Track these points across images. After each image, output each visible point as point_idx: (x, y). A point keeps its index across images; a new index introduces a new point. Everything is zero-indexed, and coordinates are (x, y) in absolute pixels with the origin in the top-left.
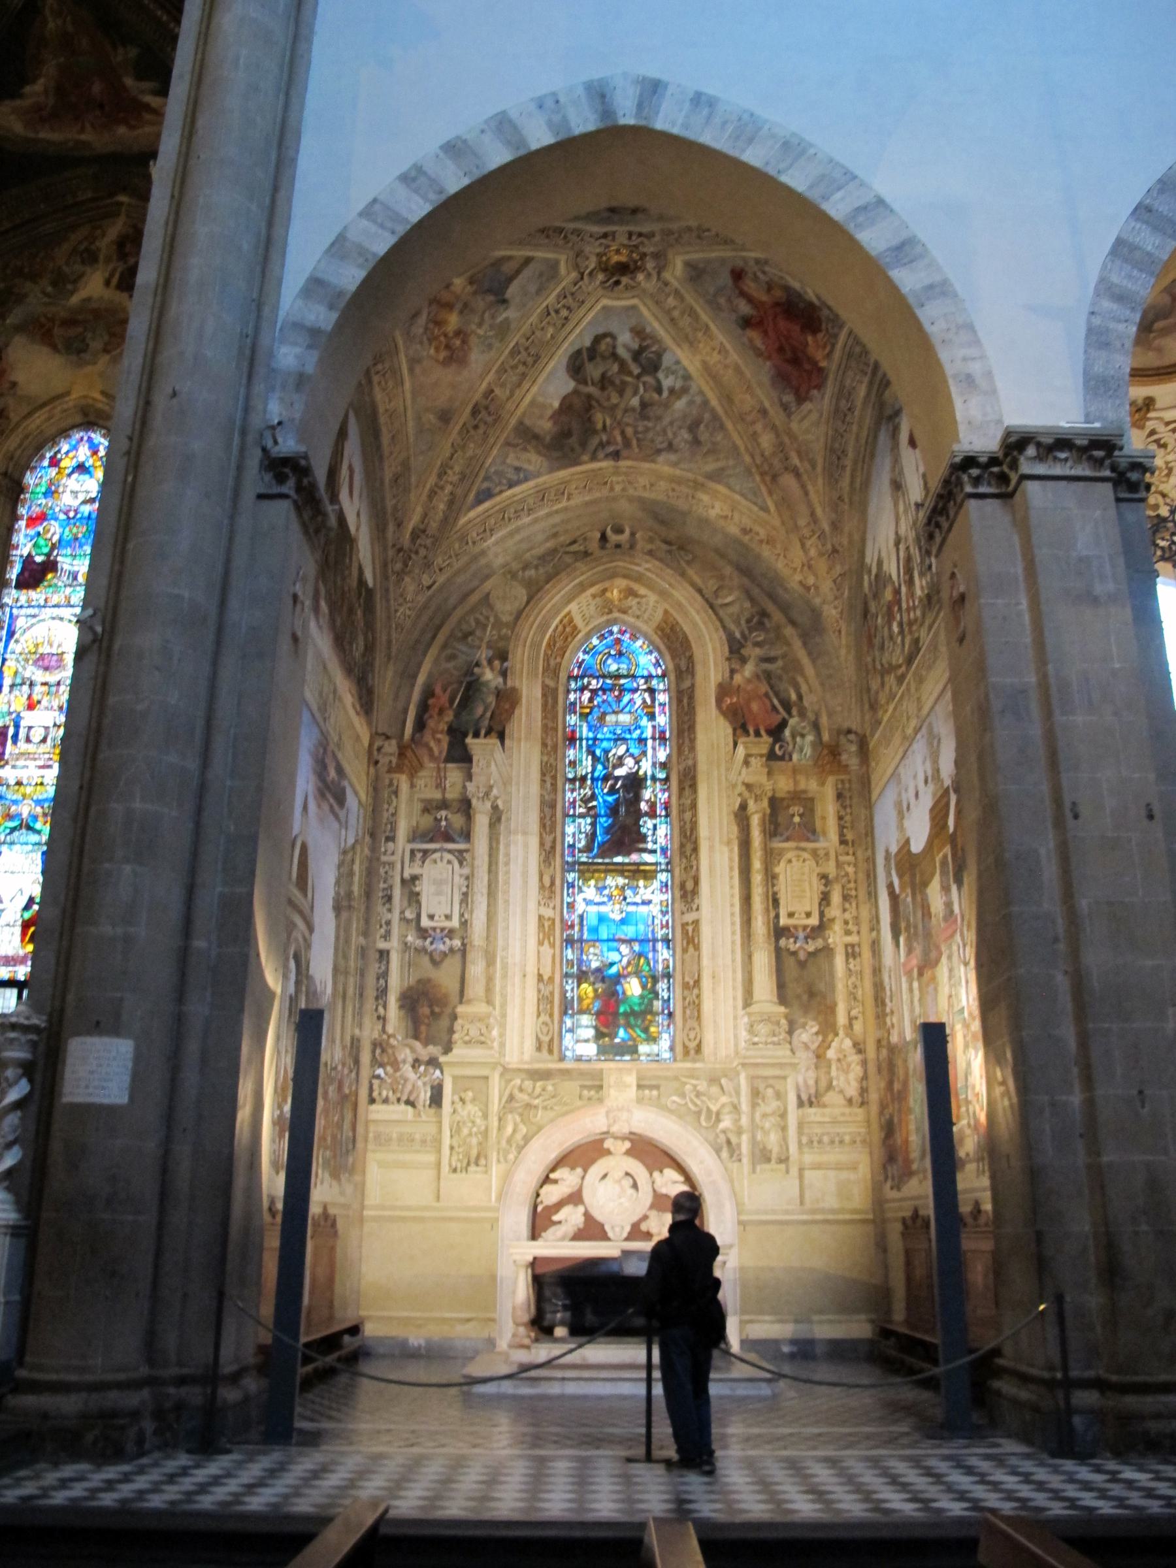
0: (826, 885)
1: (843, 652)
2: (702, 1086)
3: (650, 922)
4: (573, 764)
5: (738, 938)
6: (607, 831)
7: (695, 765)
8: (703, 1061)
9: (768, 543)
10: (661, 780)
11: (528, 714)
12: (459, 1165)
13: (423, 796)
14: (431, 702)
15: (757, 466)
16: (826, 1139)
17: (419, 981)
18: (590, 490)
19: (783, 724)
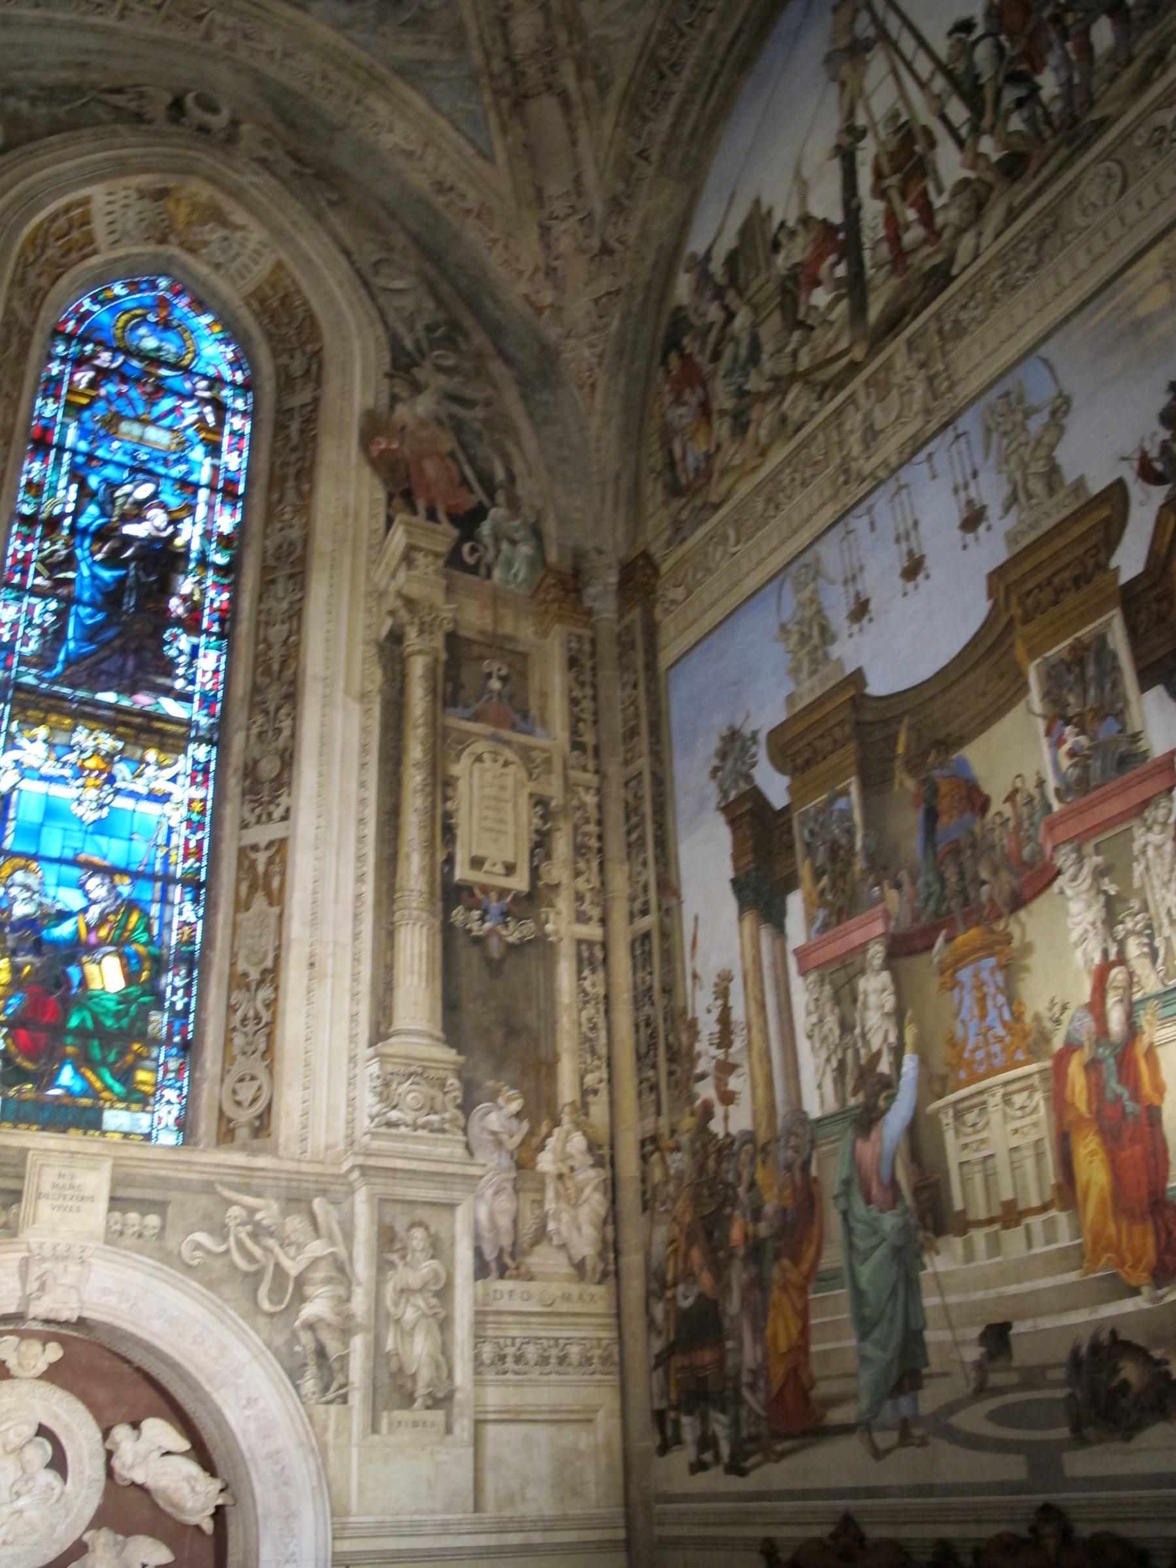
0: (544, 818)
1: (595, 422)
2: (268, 1211)
3: (161, 840)
4: (35, 488)
5: (369, 889)
6: (90, 634)
7: (306, 539)
8: (274, 1151)
9: (478, 217)
10: (218, 569)
15: (492, 76)
16: (531, 1352)
18: (169, 18)
19: (479, 514)
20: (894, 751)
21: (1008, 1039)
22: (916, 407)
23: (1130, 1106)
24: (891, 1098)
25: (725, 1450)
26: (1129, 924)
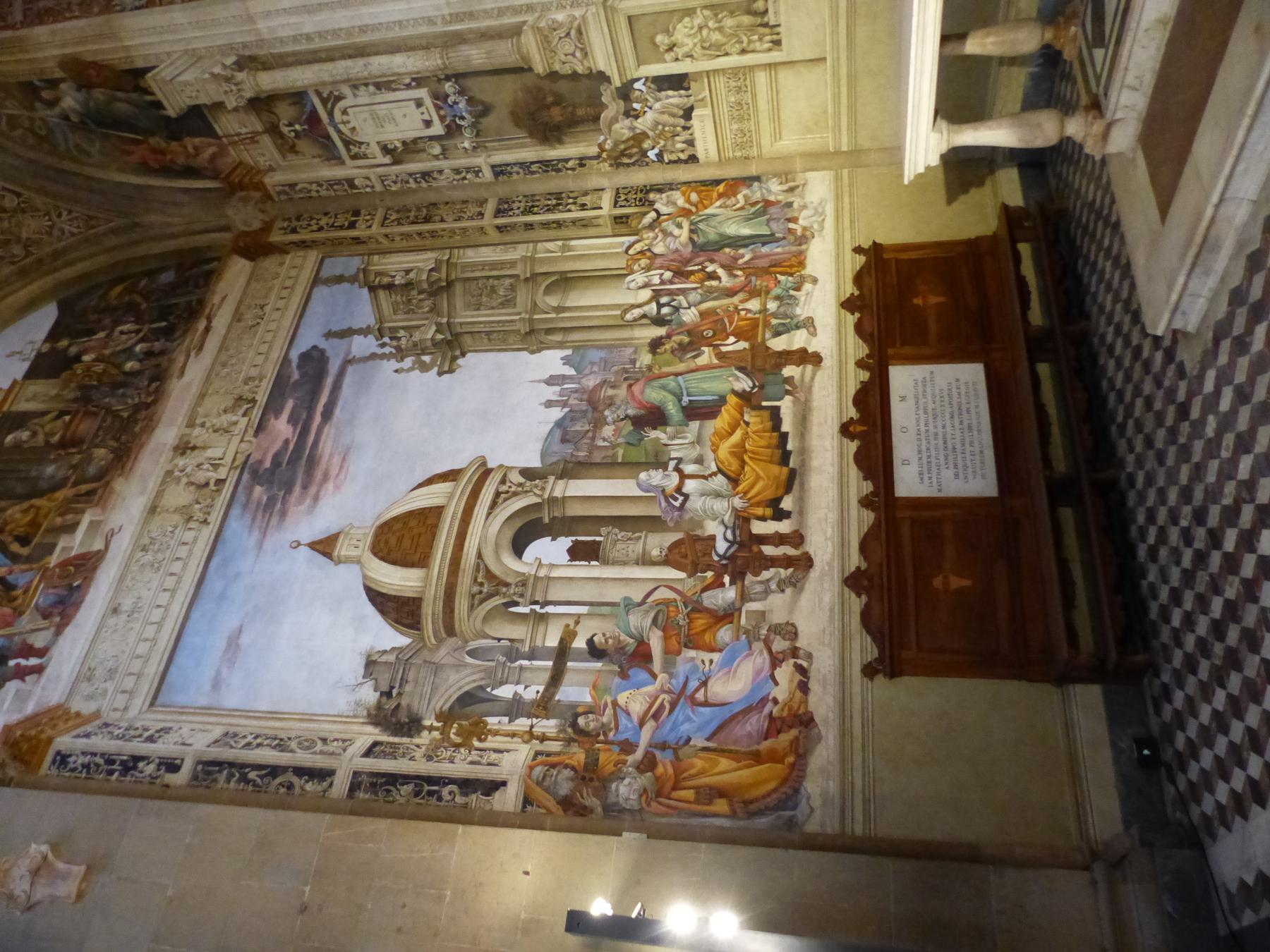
11: (83, 40)
12: (768, 38)
13: (277, 156)
14: (156, 166)
17: (518, 123)
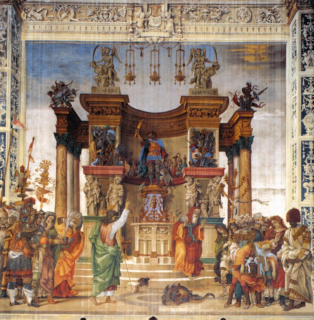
20: (137, 127)
21: (161, 215)
22: (166, 29)
23: (194, 239)
24: (117, 219)
25: (29, 300)
26: (203, 201)
